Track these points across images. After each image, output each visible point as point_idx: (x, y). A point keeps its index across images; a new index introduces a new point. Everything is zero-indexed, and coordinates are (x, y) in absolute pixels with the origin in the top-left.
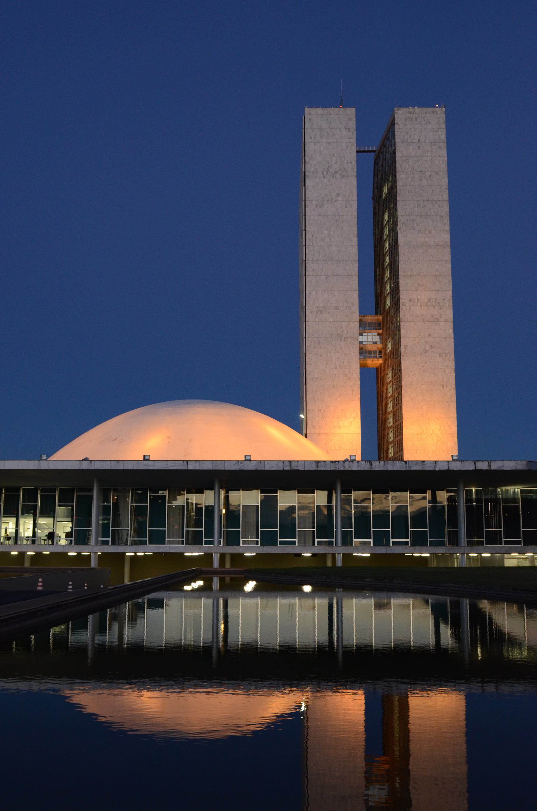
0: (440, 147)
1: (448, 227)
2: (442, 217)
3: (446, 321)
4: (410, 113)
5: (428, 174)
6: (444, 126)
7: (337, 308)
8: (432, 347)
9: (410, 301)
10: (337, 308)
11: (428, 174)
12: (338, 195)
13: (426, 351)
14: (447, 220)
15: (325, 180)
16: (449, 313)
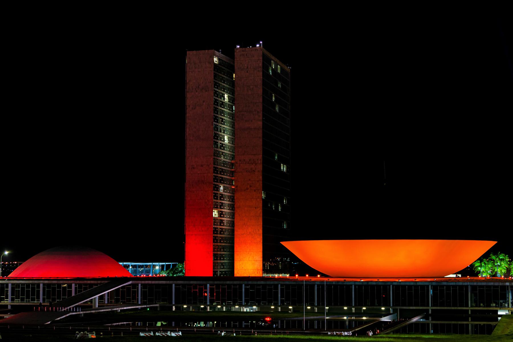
0: (259, 71)
1: (261, 118)
2: (258, 112)
3: (258, 172)
4: (243, 51)
5: (251, 87)
6: (261, 58)
7: (202, 166)
8: (250, 186)
9: (240, 161)
10: (202, 166)
11: (251, 87)
12: (204, 102)
13: (247, 189)
14: (261, 114)
15: (197, 93)
16: (260, 167)
